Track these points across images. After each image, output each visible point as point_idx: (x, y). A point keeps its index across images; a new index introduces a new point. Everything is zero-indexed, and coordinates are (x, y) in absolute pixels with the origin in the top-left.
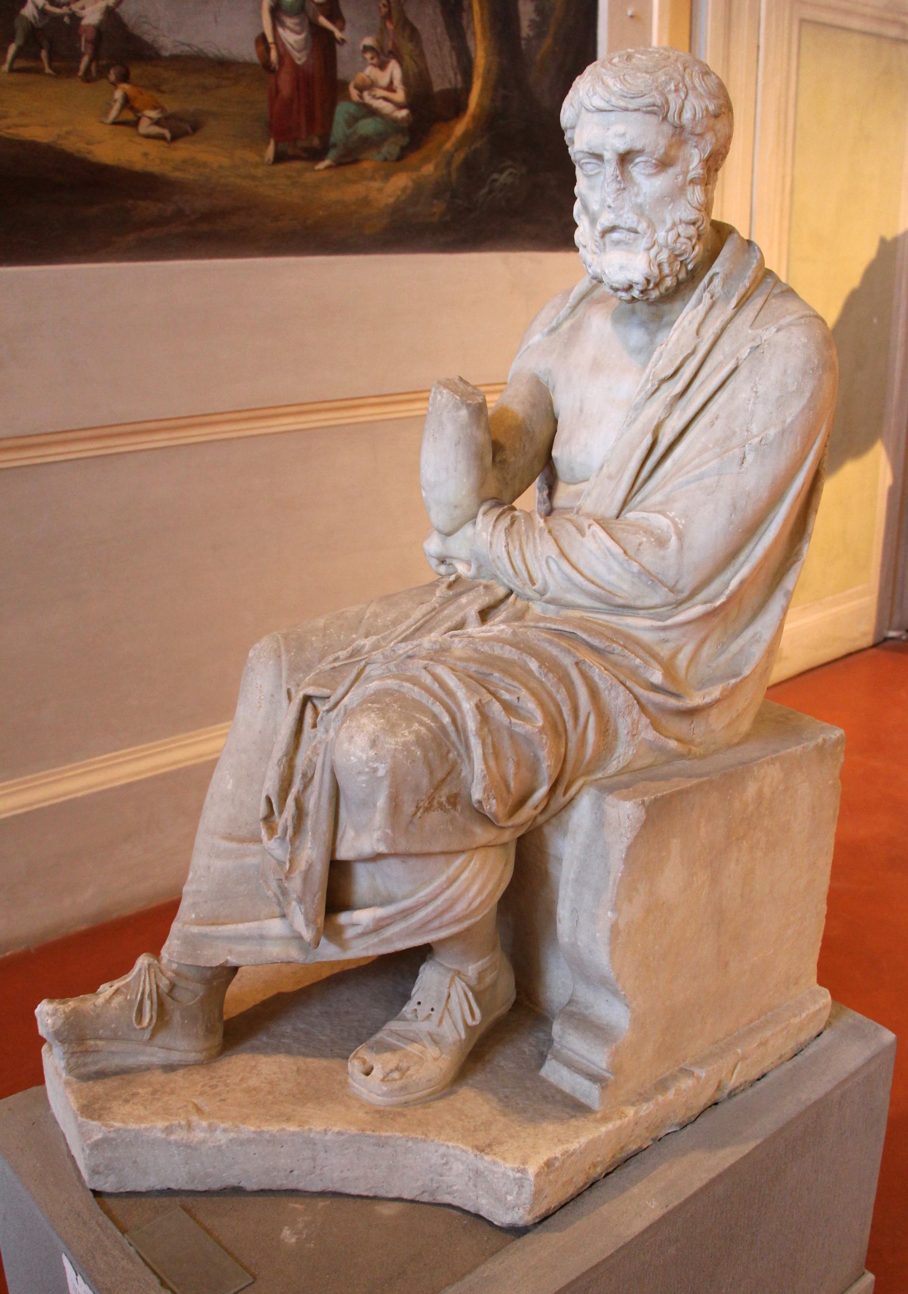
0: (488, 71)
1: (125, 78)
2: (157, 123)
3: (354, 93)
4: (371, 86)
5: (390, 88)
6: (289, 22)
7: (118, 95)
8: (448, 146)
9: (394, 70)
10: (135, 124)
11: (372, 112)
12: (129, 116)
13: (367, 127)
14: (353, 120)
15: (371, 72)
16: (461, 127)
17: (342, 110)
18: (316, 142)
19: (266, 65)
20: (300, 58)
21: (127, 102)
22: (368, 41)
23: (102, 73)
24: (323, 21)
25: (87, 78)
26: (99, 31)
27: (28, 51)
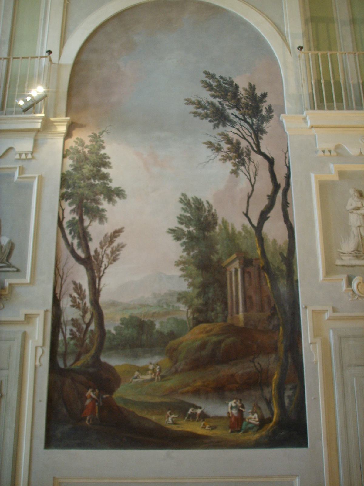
0: (277, 414)
1: (204, 421)
2: (209, 427)
3: (247, 420)
4: (250, 418)
5: (255, 418)
6: (234, 409)
7: (202, 423)
8: (268, 428)
9: (256, 415)
10: (205, 428)
11: (250, 423)
12: (204, 426)
13: (250, 426)
14: (247, 425)
15: (251, 416)
16: (271, 425)
17: (244, 423)
18: (239, 429)
19: (229, 417)
20: (236, 415)
21: (204, 425)
22: (250, 411)
23: (200, 420)
24: (241, 409)
25: (198, 421)
26: (200, 415)
27: (188, 418)
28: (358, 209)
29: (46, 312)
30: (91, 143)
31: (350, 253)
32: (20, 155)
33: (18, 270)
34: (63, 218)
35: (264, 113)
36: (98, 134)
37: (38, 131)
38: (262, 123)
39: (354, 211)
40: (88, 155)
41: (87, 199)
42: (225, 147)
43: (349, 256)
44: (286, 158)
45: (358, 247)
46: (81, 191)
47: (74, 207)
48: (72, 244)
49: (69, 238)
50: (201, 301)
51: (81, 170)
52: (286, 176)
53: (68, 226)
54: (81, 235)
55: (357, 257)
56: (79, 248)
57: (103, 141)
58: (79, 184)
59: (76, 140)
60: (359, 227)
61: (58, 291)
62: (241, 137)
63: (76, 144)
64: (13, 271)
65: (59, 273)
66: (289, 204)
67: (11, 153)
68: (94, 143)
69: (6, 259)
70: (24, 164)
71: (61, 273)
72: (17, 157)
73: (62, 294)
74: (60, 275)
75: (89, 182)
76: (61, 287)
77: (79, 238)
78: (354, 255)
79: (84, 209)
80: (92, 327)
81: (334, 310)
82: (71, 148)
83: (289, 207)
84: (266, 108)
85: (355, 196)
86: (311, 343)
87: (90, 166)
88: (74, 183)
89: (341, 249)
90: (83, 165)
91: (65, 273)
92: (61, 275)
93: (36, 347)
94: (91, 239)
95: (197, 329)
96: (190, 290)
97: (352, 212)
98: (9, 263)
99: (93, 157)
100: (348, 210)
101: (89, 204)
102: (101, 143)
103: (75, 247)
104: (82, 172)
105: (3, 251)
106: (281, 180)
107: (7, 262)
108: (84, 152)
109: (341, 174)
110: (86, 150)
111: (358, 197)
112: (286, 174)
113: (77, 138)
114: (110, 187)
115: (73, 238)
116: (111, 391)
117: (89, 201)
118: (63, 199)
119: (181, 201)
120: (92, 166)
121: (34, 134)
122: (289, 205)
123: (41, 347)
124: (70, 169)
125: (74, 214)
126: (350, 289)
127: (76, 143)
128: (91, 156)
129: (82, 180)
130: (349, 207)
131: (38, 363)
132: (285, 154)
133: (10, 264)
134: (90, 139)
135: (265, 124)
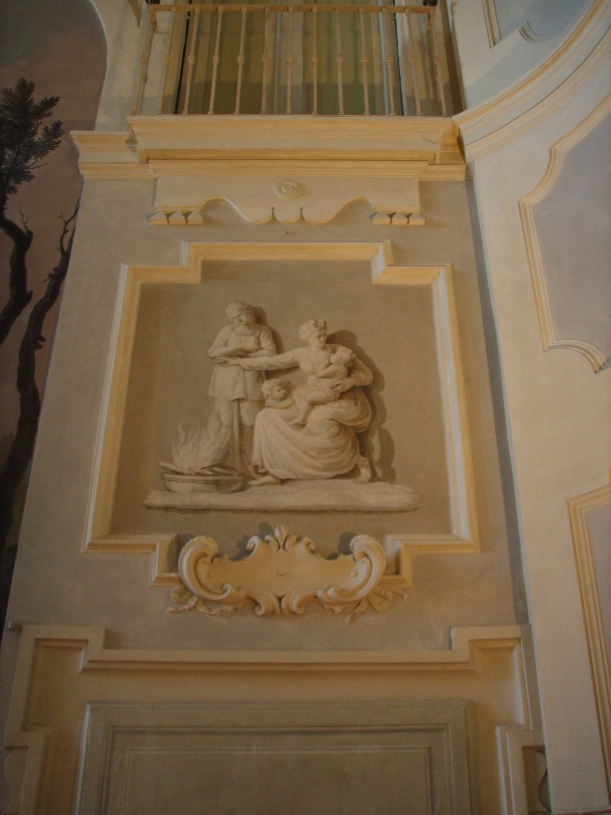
28: (244, 354)
31: (198, 474)
35: (39, 136)
38: (28, 158)
39: (231, 361)
43: (194, 482)
44: (65, 231)
45: (226, 455)
52: (53, 273)
55: (218, 486)
60: (239, 400)
66: (44, 340)
78: (211, 478)
81: (111, 641)
83: (40, 347)
84: (46, 129)
85: (240, 321)
89: (170, 460)
97: (224, 363)
100: (214, 358)
106: (37, 285)
109: (211, 270)
111: (248, 324)
112: (55, 269)
122: (41, 343)
126: (173, 575)
130: (216, 350)
132: (67, 223)
135: (32, 161)
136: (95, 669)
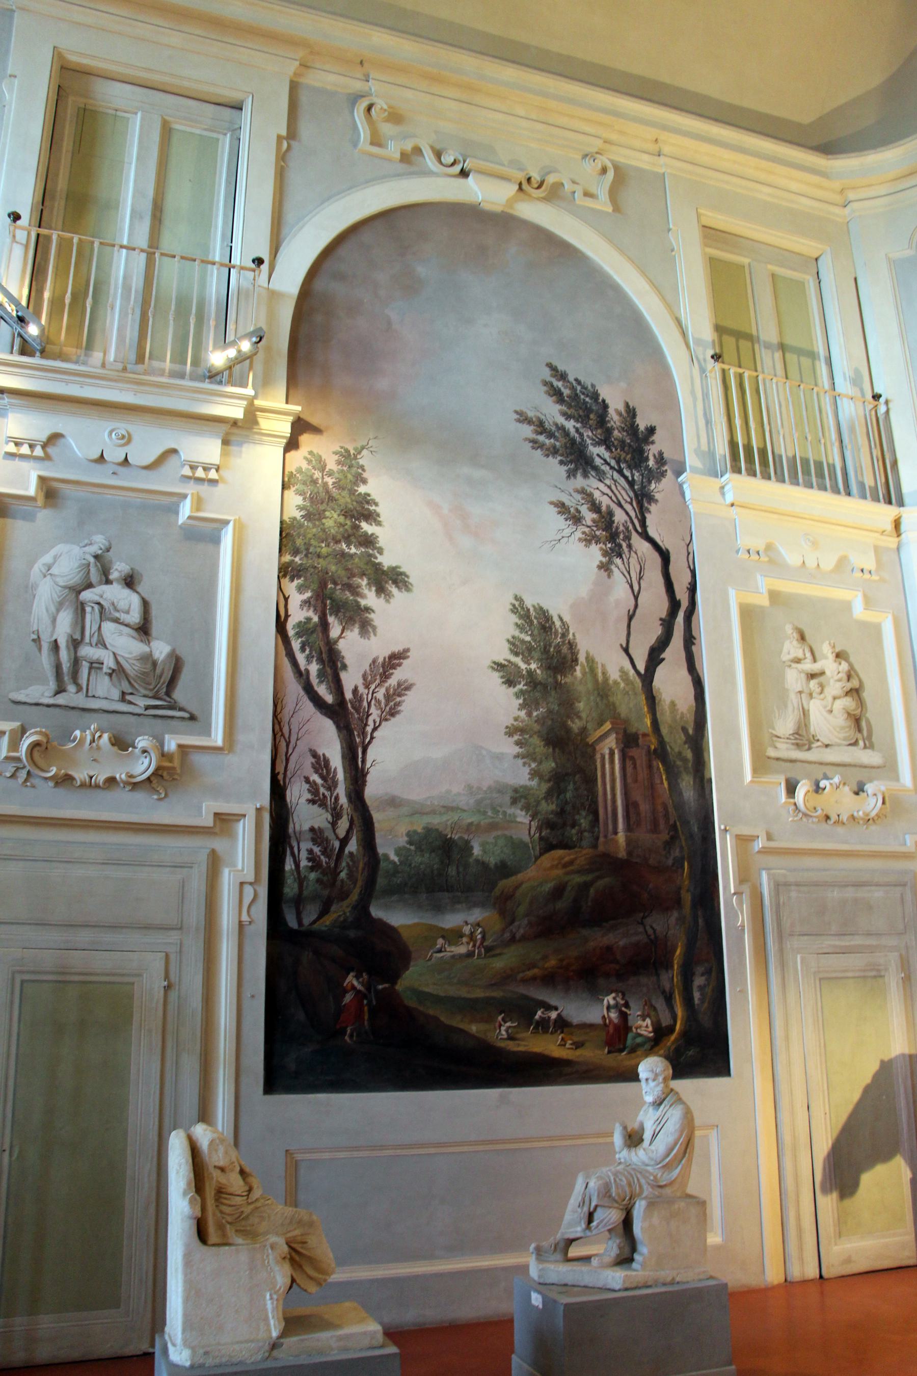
0: (683, 1017)
1: (562, 1032)
2: (571, 1044)
3: (634, 1030)
4: (640, 1027)
5: (647, 1026)
6: (613, 1011)
7: (560, 1037)
8: (669, 1044)
9: (648, 1021)
10: (565, 1045)
11: (640, 1035)
12: (563, 1043)
13: (639, 1040)
14: (634, 1038)
15: (640, 1022)
16: (673, 1037)
17: (630, 1036)
18: (622, 1046)
19: (605, 1024)
20: (616, 1021)
21: (563, 1039)
22: (639, 1013)
23: (556, 1031)
24: (623, 1009)
25: (552, 1033)
26: (556, 1020)
27: (536, 1028)
28: (798, 661)
29: (259, 810)
30: (340, 467)
31: (788, 738)
32: (193, 468)
33: (192, 718)
34: (287, 616)
35: (651, 463)
36: (352, 452)
37: (235, 423)
38: (650, 482)
39: (794, 665)
40: (335, 493)
41: (335, 583)
42: (589, 516)
43: (787, 743)
44: (689, 554)
45: (799, 728)
46: (321, 564)
47: (308, 594)
48: (307, 671)
49: (301, 658)
50: (553, 807)
51: (320, 519)
53: (298, 635)
54: (325, 656)
55: (798, 746)
56: (321, 682)
57: (362, 467)
58: (318, 550)
59: (309, 457)
60: (800, 692)
61: (280, 768)
62: (613, 501)
63: (308, 464)
64: (183, 718)
65: (281, 730)
66: (695, 639)
67: (173, 461)
68: (345, 469)
69: (164, 690)
70: (204, 489)
71: (286, 730)
72: (187, 471)
73: (289, 774)
74: (283, 735)
75: (337, 547)
76: (287, 760)
77: (320, 660)
78: (793, 741)
79: (328, 602)
80: (353, 846)
81: (769, 837)
82: (299, 470)
83: (694, 644)
84: (654, 456)
85: (794, 637)
86: (735, 894)
87: (339, 515)
88: (308, 546)
89: (774, 729)
90: (324, 511)
91: (294, 731)
92: (287, 736)
93: (242, 884)
94: (345, 667)
95: (547, 860)
96: (534, 783)
97: (790, 666)
98: (172, 700)
99: (343, 497)
100: (784, 662)
101: (338, 592)
102: (360, 471)
103: (314, 680)
104: (324, 524)
105: (158, 671)
106: (682, 595)
107: (168, 699)
108: (325, 484)
109: (774, 596)
110: (330, 481)
111: (797, 640)
112: (690, 584)
113: (311, 453)
114: (379, 564)
115: (309, 659)
116: (394, 978)
117: (339, 587)
118: (285, 576)
119: (514, 610)
120: (343, 515)
121: (224, 428)
122: (694, 641)
123: (251, 884)
124: (298, 514)
125: (308, 610)
126: (792, 800)
127: (309, 462)
128: (340, 494)
129: (323, 542)
130: (785, 657)
131: (245, 917)
132: (688, 545)
133: (175, 702)
134: (336, 457)
135: (653, 486)
136: (764, 851)
